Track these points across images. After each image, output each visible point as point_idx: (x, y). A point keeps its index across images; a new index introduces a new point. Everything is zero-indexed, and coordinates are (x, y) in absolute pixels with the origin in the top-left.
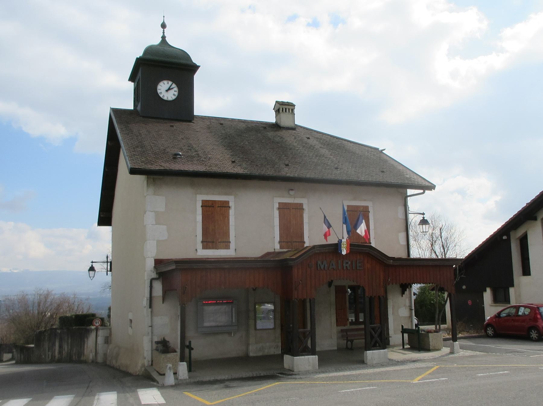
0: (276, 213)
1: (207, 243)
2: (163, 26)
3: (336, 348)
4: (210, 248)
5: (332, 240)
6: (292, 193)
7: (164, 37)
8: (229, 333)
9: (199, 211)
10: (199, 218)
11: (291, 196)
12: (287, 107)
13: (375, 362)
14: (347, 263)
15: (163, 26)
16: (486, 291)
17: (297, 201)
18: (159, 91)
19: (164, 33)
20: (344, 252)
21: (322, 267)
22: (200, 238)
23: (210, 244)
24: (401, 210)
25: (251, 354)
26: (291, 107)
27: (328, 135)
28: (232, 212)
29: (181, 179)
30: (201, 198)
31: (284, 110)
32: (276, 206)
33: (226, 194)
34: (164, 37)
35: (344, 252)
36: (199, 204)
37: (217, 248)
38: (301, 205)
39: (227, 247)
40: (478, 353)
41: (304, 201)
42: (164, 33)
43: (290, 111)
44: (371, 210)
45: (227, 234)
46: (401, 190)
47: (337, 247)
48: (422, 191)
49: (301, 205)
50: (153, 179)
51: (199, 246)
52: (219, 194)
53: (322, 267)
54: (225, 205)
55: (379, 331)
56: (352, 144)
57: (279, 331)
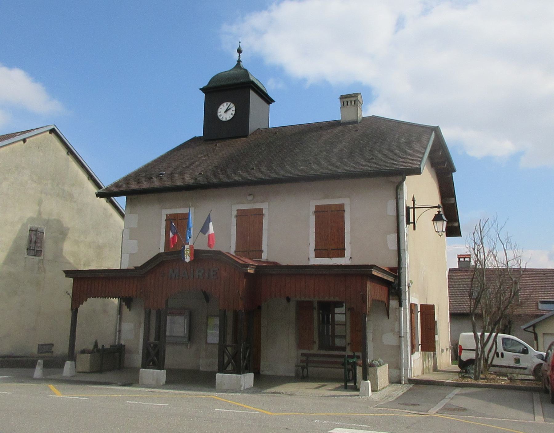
0: (234, 221)
3: (293, 375)
6: (250, 198)
7: (239, 61)
11: (250, 202)
12: (348, 99)
15: (239, 51)
18: (219, 114)
20: (188, 259)
21: (174, 276)
24: (391, 204)
25: (201, 369)
26: (353, 99)
32: (235, 213)
34: (239, 61)
35: (188, 259)
38: (261, 210)
41: (264, 206)
43: (353, 103)
44: (346, 208)
49: (261, 210)
50: (131, 200)
53: (174, 276)
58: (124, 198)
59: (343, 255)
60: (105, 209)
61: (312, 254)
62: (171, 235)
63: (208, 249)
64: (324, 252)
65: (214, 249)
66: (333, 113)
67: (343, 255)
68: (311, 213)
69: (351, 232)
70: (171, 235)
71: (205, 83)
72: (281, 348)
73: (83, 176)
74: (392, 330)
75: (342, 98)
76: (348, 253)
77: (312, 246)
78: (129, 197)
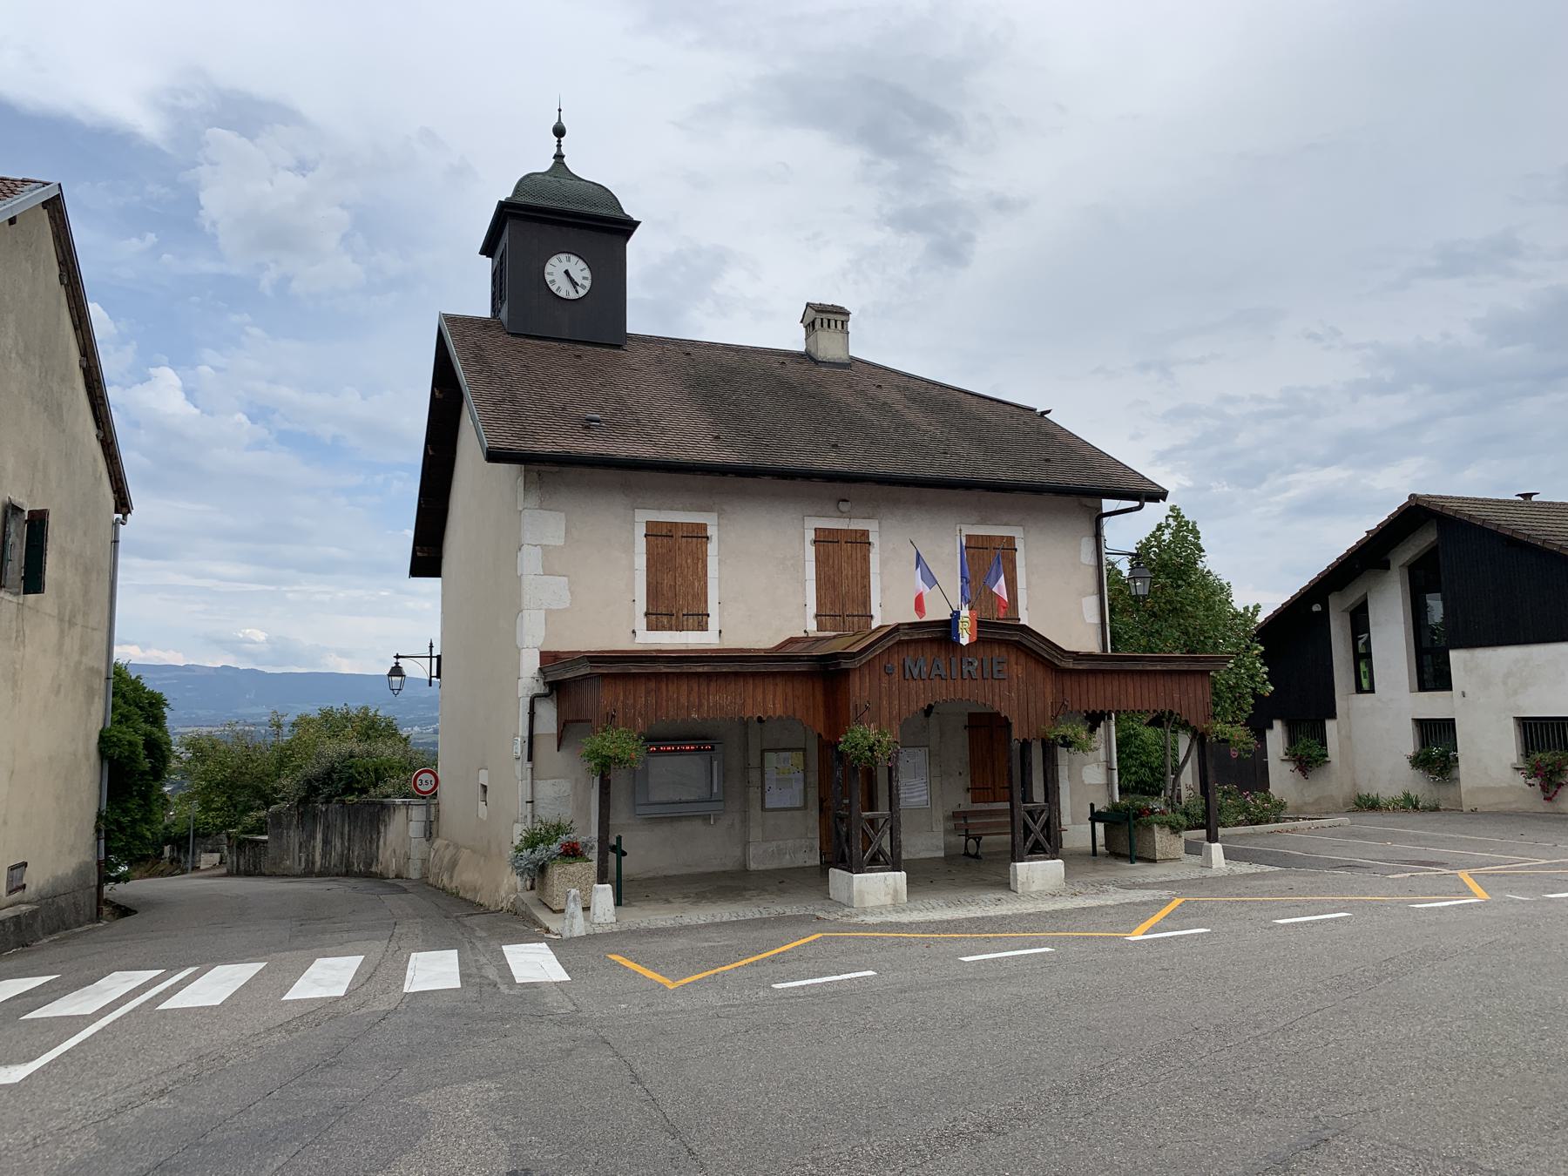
0: (810, 552)
1: (656, 619)
2: (559, 132)
4: (663, 628)
5: (937, 611)
6: (844, 507)
7: (559, 157)
8: (706, 818)
9: (641, 544)
10: (641, 561)
11: (842, 515)
12: (831, 316)
13: (1034, 888)
14: (971, 663)
15: (559, 132)
16: (1271, 727)
17: (857, 525)
18: (548, 278)
19: (559, 146)
22: (641, 606)
23: (665, 620)
24: (1087, 546)
25: (753, 866)
26: (840, 318)
27: (922, 379)
28: (712, 548)
29: (599, 473)
30: (643, 517)
32: (810, 535)
33: (701, 509)
34: (559, 157)
35: (965, 640)
36: (641, 530)
37: (679, 628)
38: (865, 533)
39: (703, 627)
40: (1268, 869)
41: (871, 526)
42: (559, 146)
44: (1019, 545)
45: (702, 596)
46: (1088, 501)
47: (948, 628)
48: (1137, 504)
49: (865, 533)
51: (641, 622)
54: (699, 535)
55: (1044, 817)
57: (814, 813)
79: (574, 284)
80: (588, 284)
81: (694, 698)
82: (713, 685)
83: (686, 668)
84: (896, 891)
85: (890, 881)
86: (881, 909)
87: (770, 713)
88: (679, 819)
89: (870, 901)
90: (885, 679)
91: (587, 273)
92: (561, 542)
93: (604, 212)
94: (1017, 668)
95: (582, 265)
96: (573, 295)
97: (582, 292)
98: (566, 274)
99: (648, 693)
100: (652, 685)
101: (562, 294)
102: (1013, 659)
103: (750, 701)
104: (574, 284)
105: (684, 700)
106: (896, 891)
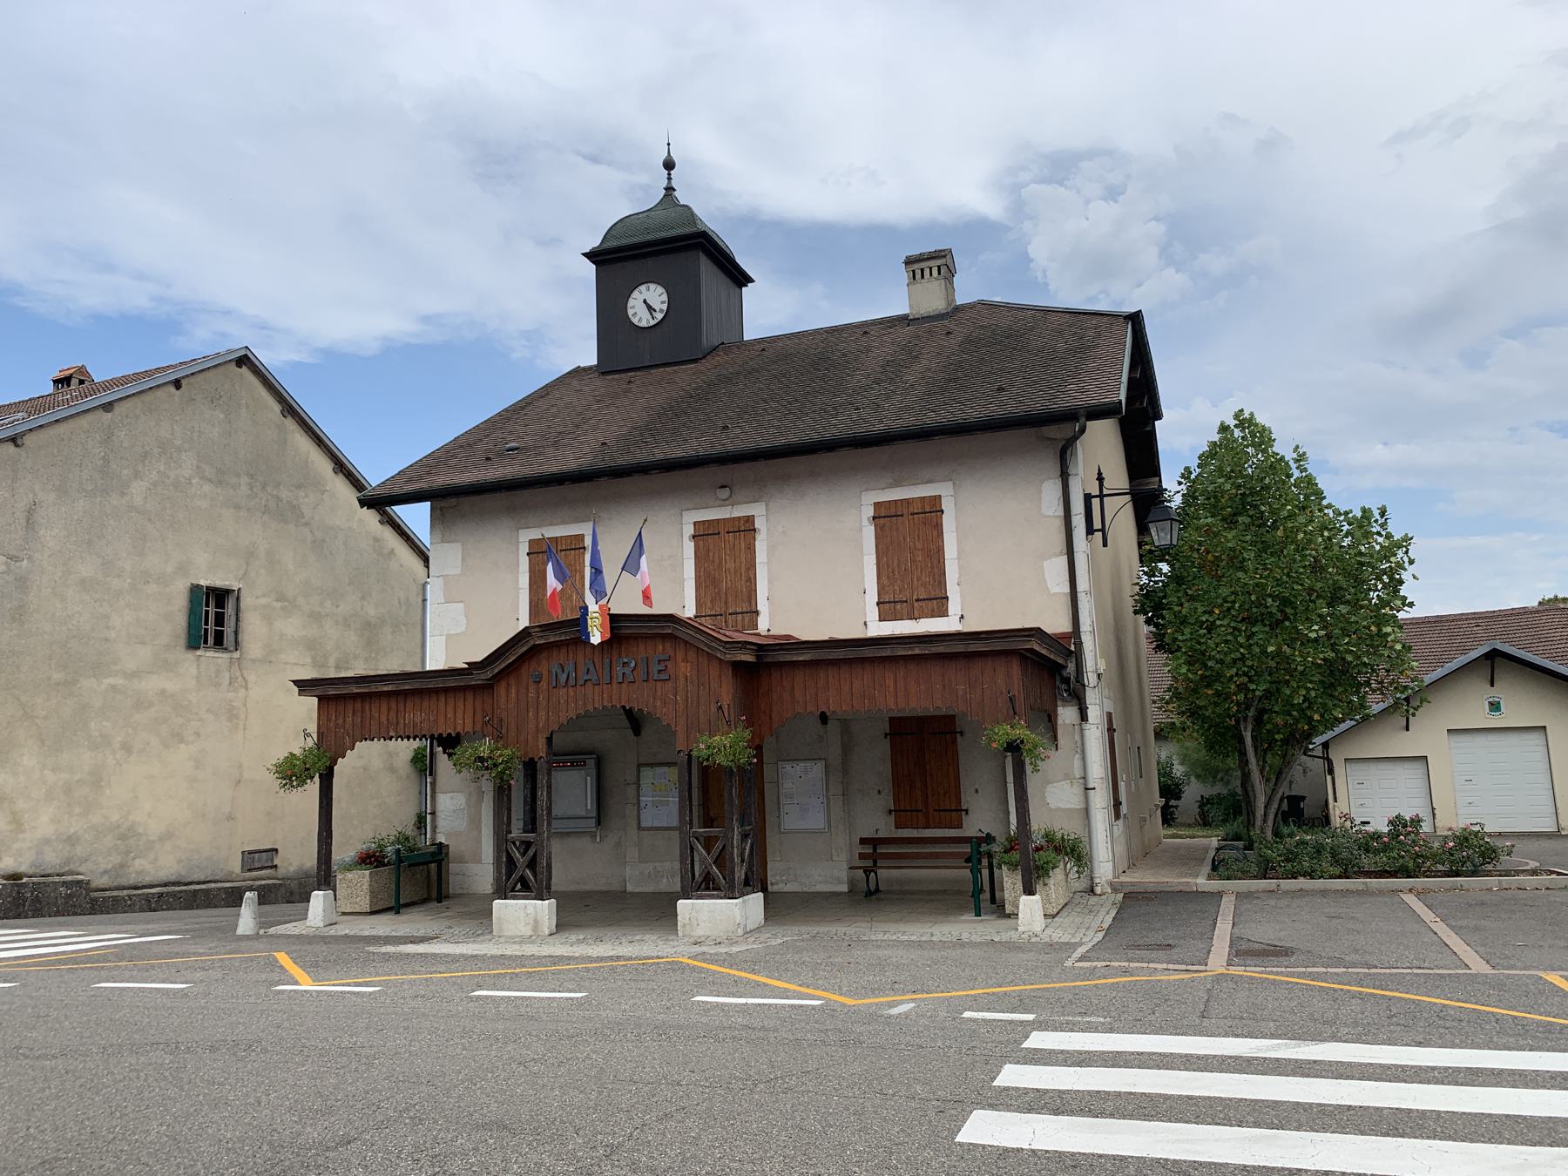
0: (689, 548)
2: (669, 165)
3: (844, 888)
6: (725, 493)
7: (670, 189)
11: (724, 503)
12: (923, 265)
15: (669, 165)
18: (630, 312)
19: (669, 179)
20: (596, 639)
25: (630, 888)
31: (918, 276)
32: (689, 530)
34: (670, 189)
35: (596, 639)
38: (750, 520)
41: (757, 510)
42: (669, 179)
44: (947, 505)
49: (750, 520)
52: (564, 522)
53: (563, 678)
55: (719, 845)
56: (1105, 319)
58: (426, 506)
59: (944, 613)
60: (376, 540)
61: (873, 612)
62: (552, 583)
63: (645, 610)
64: (898, 606)
65: (657, 610)
66: (892, 299)
67: (944, 613)
68: (865, 522)
69: (959, 558)
70: (552, 583)
71: (594, 242)
72: (815, 825)
73: (324, 466)
74: (1067, 776)
75: (909, 262)
76: (954, 606)
77: (872, 596)
78: (444, 503)
79: (650, 308)
80: (665, 307)
81: (392, 715)
82: (409, 705)
83: (374, 688)
84: (536, 921)
85: (530, 910)
86: (513, 940)
87: (459, 729)
88: (568, 834)
89: (510, 930)
90: (532, 689)
91: (665, 297)
92: (457, 571)
93: (688, 230)
94: (684, 668)
95: (660, 290)
96: (652, 323)
97: (659, 316)
98: (648, 303)
99: (354, 713)
100: (358, 705)
101: (644, 324)
102: (680, 655)
103: (442, 719)
104: (650, 308)
105: (384, 719)
106: (536, 921)
